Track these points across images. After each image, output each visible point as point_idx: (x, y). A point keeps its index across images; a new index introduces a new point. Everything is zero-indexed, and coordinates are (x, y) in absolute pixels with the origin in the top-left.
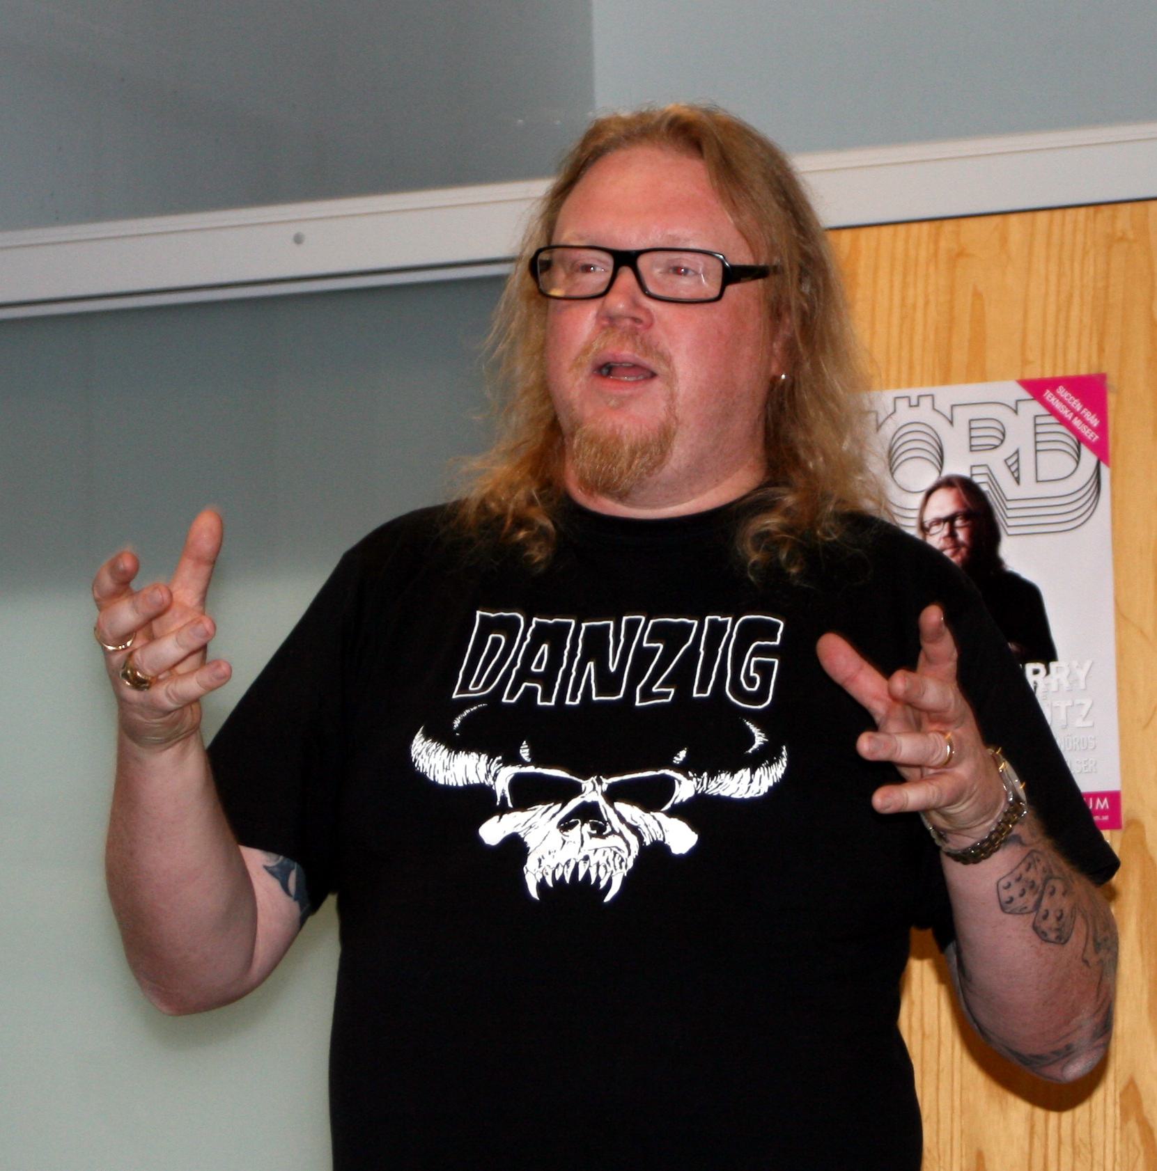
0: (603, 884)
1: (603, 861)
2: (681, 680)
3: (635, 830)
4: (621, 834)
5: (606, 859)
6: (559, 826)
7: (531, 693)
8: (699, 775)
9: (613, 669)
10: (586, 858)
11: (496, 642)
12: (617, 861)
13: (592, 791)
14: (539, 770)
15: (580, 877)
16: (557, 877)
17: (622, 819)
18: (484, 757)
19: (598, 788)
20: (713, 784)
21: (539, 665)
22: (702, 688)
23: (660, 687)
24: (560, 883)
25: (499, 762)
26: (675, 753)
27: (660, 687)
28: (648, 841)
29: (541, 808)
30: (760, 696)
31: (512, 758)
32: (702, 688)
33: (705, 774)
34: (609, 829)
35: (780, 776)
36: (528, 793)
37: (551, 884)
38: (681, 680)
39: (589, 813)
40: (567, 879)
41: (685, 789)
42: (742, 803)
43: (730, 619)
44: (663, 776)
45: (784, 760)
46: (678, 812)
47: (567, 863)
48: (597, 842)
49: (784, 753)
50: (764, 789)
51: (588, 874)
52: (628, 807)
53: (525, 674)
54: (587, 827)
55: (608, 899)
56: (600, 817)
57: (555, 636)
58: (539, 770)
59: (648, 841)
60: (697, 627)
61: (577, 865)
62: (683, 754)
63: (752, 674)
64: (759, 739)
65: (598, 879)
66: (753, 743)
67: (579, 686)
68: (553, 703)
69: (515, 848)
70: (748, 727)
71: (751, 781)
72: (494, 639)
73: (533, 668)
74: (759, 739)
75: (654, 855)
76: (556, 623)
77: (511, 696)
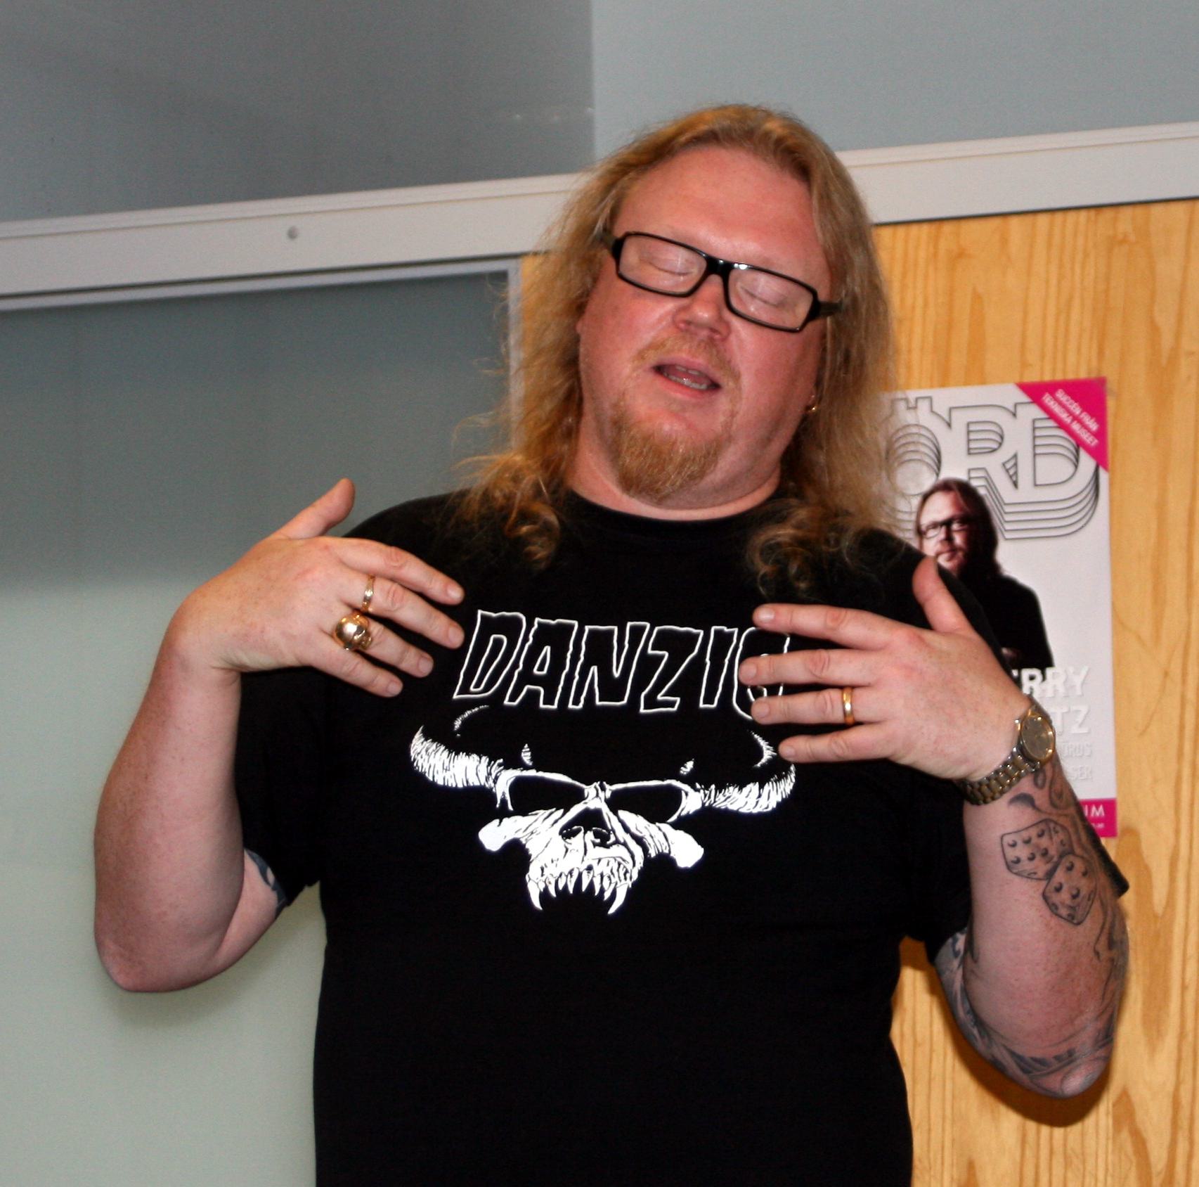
0: (607, 895)
1: (607, 872)
2: (687, 688)
3: (639, 841)
4: (625, 844)
5: (611, 870)
6: (561, 833)
7: (533, 696)
8: (707, 788)
9: (617, 674)
10: (590, 868)
11: (498, 643)
12: (622, 872)
13: (595, 798)
14: (541, 774)
15: (584, 887)
16: (561, 887)
17: (627, 829)
18: (485, 760)
19: (601, 794)
20: (721, 797)
21: (541, 669)
22: (709, 700)
24: (563, 893)
25: (500, 765)
26: (683, 764)
28: (653, 853)
29: (542, 813)
31: (513, 762)
32: (709, 700)
33: (713, 787)
34: (613, 839)
35: (788, 792)
36: (529, 798)
38: (687, 688)
39: (591, 820)
41: (692, 801)
42: (750, 816)
43: (736, 630)
44: (670, 787)
45: (793, 776)
47: (571, 873)
48: (601, 851)
50: (773, 805)
51: (591, 885)
52: (633, 815)
53: (527, 677)
54: (590, 835)
55: (612, 910)
56: (603, 825)
57: (556, 637)
58: (541, 774)
59: (653, 853)
60: (703, 637)
61: (580, 875)
62: (690, 765)
65: (602, 891)
66: (761, 757)
67: (581, 690)
68: (555, 706)
69: (516, 854)
70: (756, 741)
71: (760, 796)
73: (535, 671)
75: (659, 868)
77: (512, 699)
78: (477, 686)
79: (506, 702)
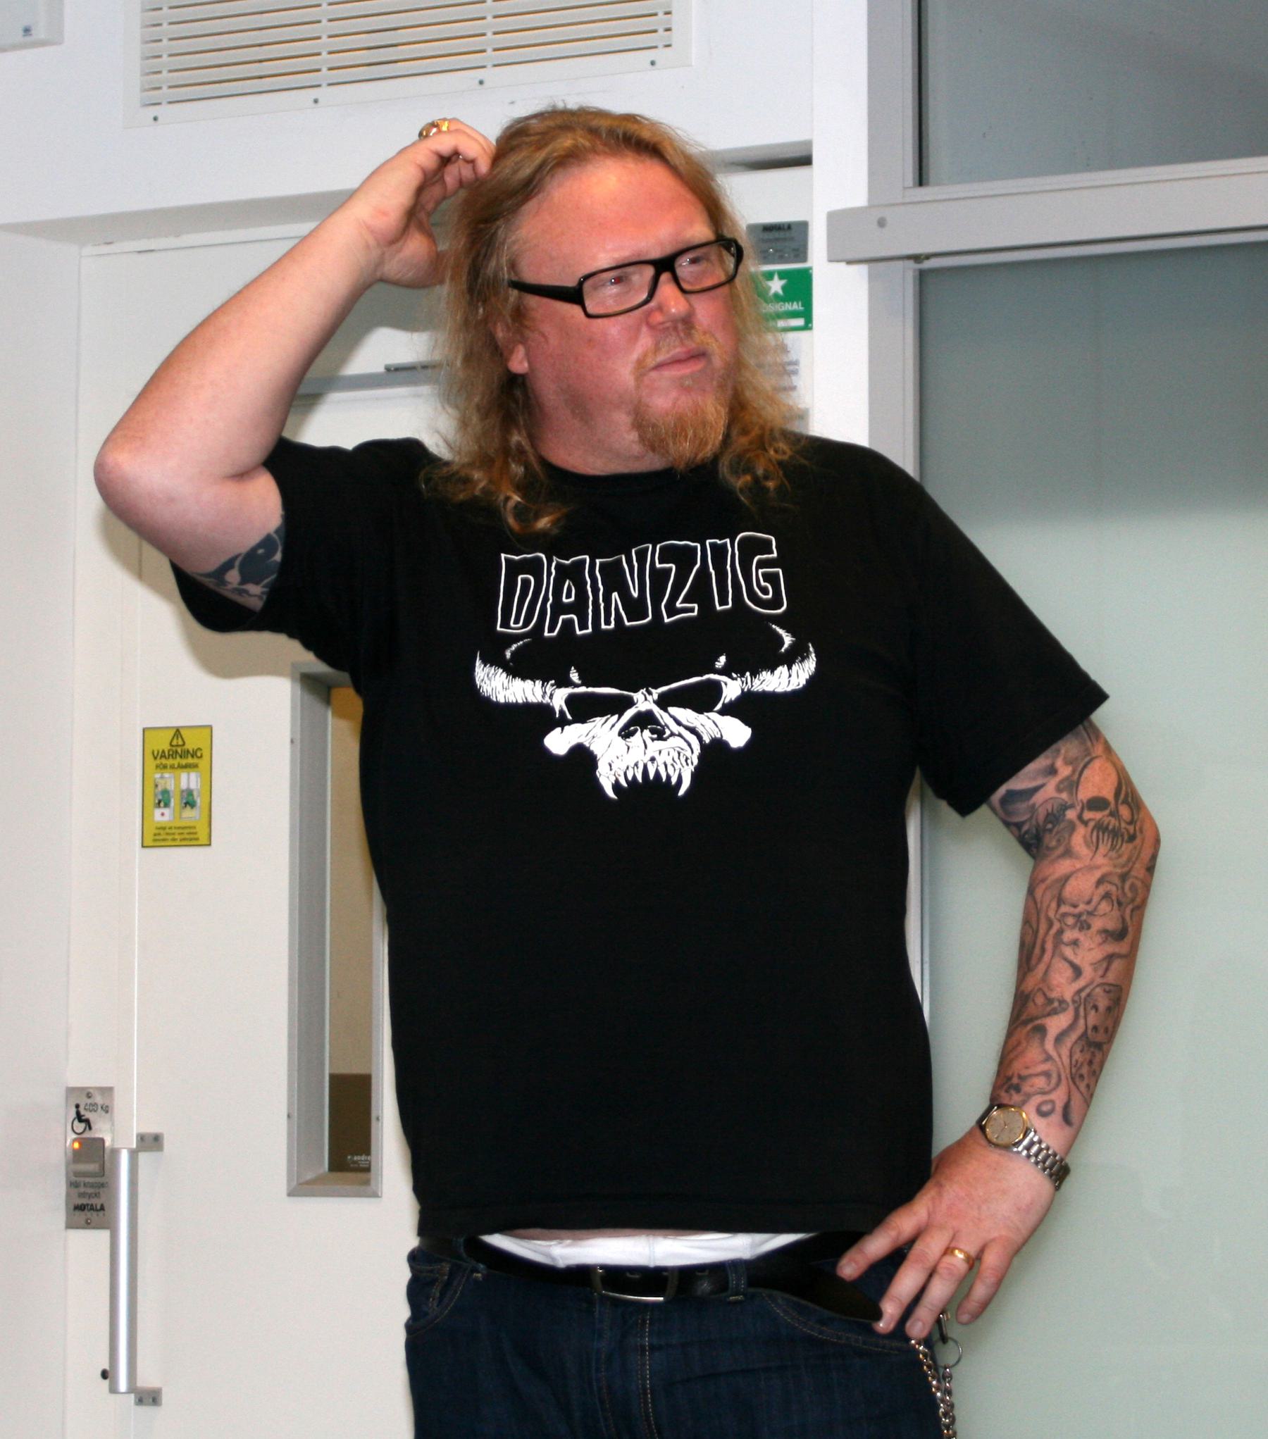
0: (674, 780)
1: (669, 762)
2: (700, 593)
3: (693, 731)
4: (680, 735)
5: (674, 759)
6: (620, 734)
7: (568, 624)
8: (743, 675)
9: (635, 595)
10: (653, 759)
11: (526, 583)
12: (683, 760)
13: (644, 701)
14: (591, 690)
15: (652, 776)
16: (630, 778)
17: (679, 723)
18: (539, 683)
19: (649, 697)
20: (756, 682)
21: (569, 596)
22: (723, 601)
24: (633, 782)
26: (716, 659)
28: (707, 740)
29: (599, 720)
30: (776, 603)
31: (564, 682)
32: (723, 601)
34: (668, 733)
36: (582, 710)
37: (625, 785)
38: (700, 593)
39: (645, 720)
40: (640, 780)
41: (732, 689)
42: (785, 695)
43: (728, 540)
44: (709, 681)
46: (728, 710)
47: (636, 765)
48: (659, 744)
50: (803, 682)
51: (657, 774)
52: (681, 710)
53: (559, 608)
54: (647, 733)
55: (681, 792)
56: (658, 723)
57: (574, 573)
58: (591, 690)
59: (707, 740)
60: (703, 549)
61: (645, 766)
62: (723, 659)
63: (763, 583)
64: (788, 640)
65: (669, 777)
66: (781, 641)
67: (611, 614)
68: (590, 630)
69: (583, 758)
70: (775, 631)
72: (523, 580)
73: (565, 600)
74: (788, 640)
75: (714, 751)
77: (551, 630)
78: (517, 622)
79: (546, 634)
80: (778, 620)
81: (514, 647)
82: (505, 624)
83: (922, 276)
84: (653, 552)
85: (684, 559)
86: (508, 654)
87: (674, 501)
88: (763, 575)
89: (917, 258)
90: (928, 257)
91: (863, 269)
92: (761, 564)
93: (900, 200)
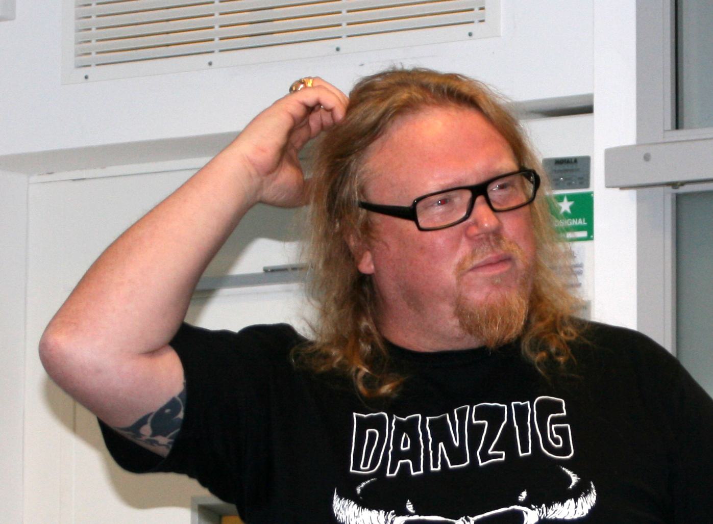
2: (507, 443)
7: (405, 467)
8: (540, 506)
9: (457, 444)
11: (372, 435)
14: (422, 517)
20: (550, 512)
21: (405, 445)
22: (525, 450)
23: (493, 450)
25: (393, 514)
26: (519, 494)
27: (493, 450)
30: (565, 451)
32: (525, 450)
33: (544, 505)
35: (594, 502)
38: (507, 443)
43: (528, 403)
44: (514, 511)
45: (594, 491)
49: (593, 486)
50: (586, 512)
53: (398, 455)
58: (422, 517)
60: (509, 409)
62: (524, 494)
63: (555, 436)
64: (575, 479)
66: (570, 482)
67: (438, 458)
68: (422, 472)
71: (576, 507)
72: (370, 433)
73: (402, 448)
74: (575, 479)
76: (409, 419)
77: (392, 471)
78: (365, 465)
79: (388, 475)
80: (567, 464)
81: (363, 485)
82: (356, 467)
83: (678, 198)
84: (471, 411)
85: (494, 417)
86: (359, 490)
87: (488, 371)
88: (556, 429)
89: (674, 185)
90: (683, 184)
91: (633, 193)
92: (554, 421)
93: (661, 140)
